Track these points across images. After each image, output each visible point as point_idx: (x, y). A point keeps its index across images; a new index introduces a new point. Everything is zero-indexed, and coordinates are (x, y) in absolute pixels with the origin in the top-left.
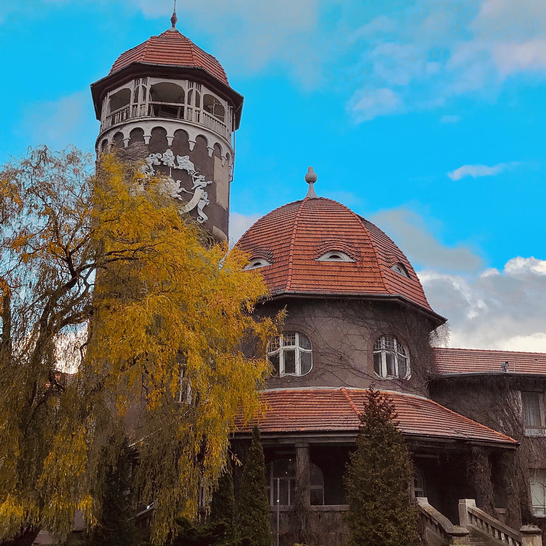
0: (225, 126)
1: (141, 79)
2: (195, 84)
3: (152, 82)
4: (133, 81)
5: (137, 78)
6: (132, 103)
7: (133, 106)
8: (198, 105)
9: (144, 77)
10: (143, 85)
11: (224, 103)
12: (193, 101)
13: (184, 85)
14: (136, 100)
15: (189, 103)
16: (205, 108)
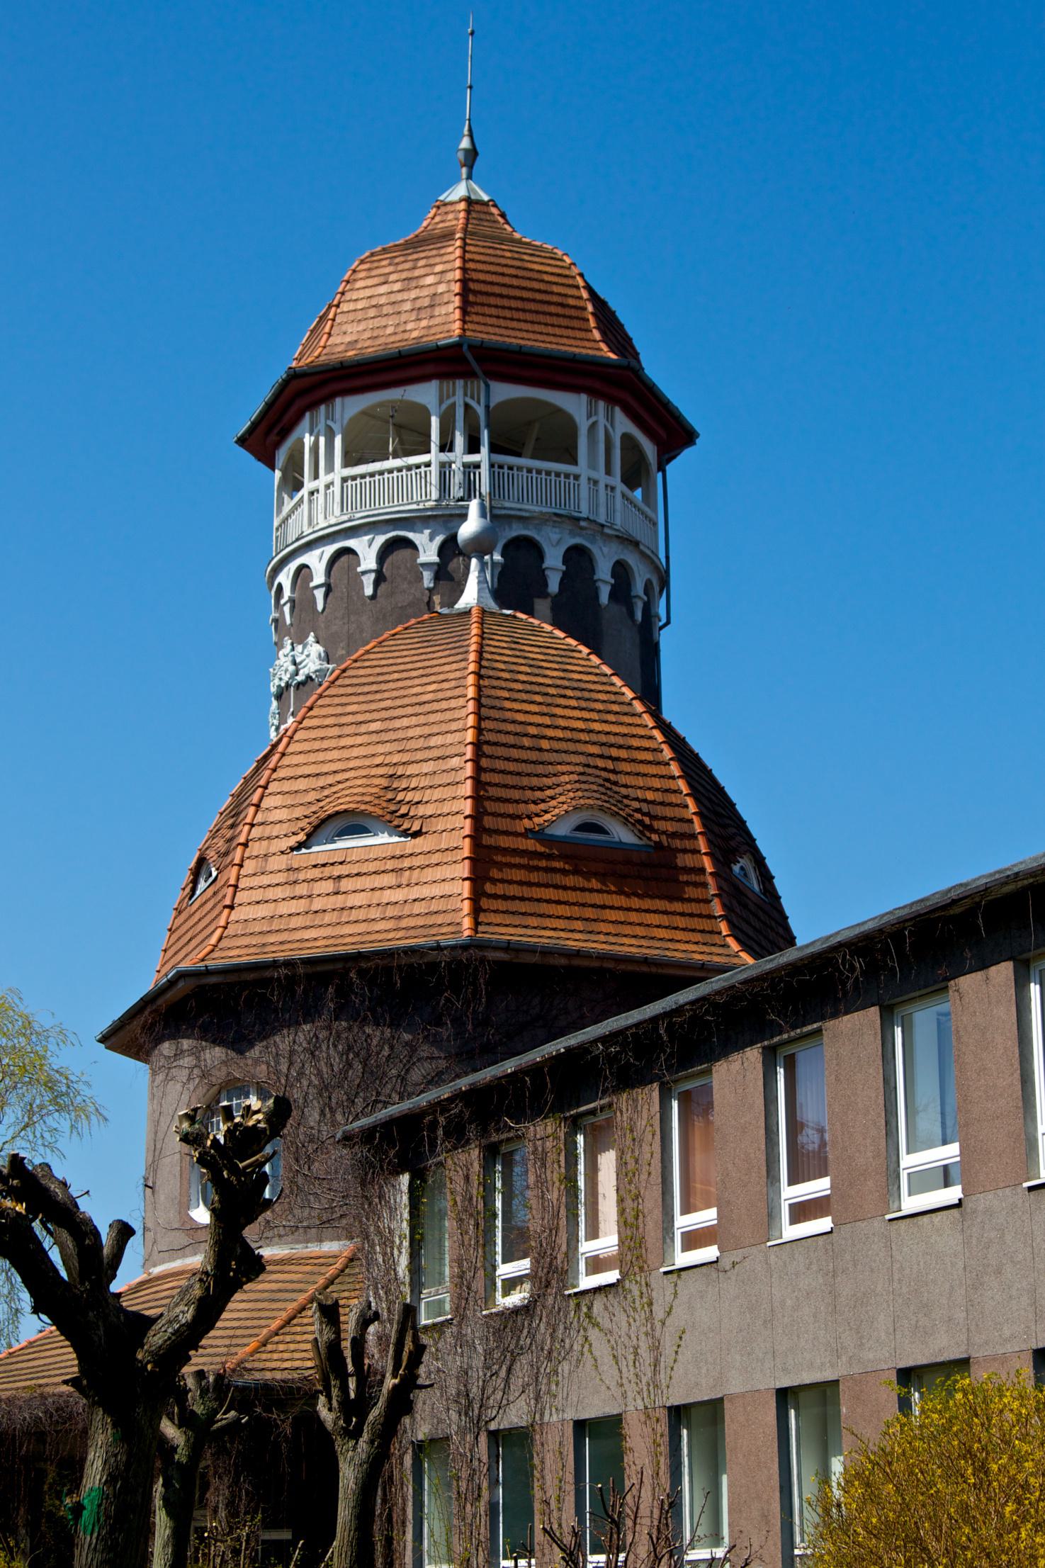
0: (577, 477)
1: (323, 408)
2: (460, 383)
3: (351, 407)
4: (308, 415)
5: (313, 406)
6: (309, 485)
7: (312, 493)
8: (473, 447)
9: (328, 399)
10: (329, 423)
11: (574, 404)
12: (459, 441)
13: (425, 394)
14: (316, 477)
15: (447, 446)
16: (494, 449)
